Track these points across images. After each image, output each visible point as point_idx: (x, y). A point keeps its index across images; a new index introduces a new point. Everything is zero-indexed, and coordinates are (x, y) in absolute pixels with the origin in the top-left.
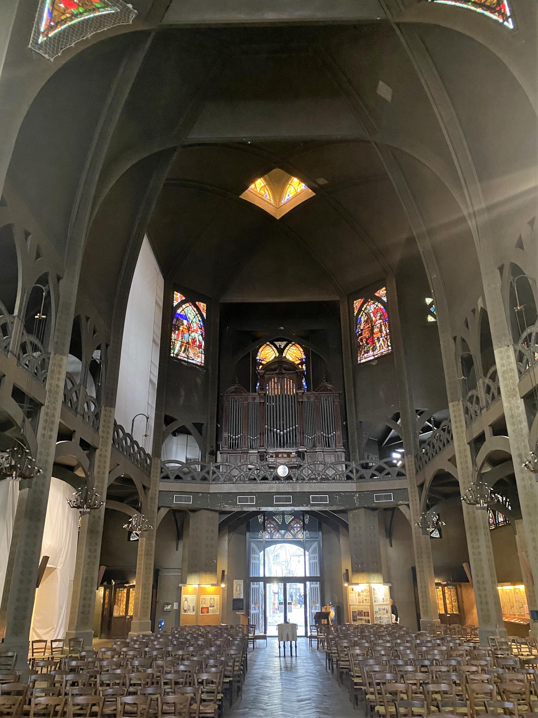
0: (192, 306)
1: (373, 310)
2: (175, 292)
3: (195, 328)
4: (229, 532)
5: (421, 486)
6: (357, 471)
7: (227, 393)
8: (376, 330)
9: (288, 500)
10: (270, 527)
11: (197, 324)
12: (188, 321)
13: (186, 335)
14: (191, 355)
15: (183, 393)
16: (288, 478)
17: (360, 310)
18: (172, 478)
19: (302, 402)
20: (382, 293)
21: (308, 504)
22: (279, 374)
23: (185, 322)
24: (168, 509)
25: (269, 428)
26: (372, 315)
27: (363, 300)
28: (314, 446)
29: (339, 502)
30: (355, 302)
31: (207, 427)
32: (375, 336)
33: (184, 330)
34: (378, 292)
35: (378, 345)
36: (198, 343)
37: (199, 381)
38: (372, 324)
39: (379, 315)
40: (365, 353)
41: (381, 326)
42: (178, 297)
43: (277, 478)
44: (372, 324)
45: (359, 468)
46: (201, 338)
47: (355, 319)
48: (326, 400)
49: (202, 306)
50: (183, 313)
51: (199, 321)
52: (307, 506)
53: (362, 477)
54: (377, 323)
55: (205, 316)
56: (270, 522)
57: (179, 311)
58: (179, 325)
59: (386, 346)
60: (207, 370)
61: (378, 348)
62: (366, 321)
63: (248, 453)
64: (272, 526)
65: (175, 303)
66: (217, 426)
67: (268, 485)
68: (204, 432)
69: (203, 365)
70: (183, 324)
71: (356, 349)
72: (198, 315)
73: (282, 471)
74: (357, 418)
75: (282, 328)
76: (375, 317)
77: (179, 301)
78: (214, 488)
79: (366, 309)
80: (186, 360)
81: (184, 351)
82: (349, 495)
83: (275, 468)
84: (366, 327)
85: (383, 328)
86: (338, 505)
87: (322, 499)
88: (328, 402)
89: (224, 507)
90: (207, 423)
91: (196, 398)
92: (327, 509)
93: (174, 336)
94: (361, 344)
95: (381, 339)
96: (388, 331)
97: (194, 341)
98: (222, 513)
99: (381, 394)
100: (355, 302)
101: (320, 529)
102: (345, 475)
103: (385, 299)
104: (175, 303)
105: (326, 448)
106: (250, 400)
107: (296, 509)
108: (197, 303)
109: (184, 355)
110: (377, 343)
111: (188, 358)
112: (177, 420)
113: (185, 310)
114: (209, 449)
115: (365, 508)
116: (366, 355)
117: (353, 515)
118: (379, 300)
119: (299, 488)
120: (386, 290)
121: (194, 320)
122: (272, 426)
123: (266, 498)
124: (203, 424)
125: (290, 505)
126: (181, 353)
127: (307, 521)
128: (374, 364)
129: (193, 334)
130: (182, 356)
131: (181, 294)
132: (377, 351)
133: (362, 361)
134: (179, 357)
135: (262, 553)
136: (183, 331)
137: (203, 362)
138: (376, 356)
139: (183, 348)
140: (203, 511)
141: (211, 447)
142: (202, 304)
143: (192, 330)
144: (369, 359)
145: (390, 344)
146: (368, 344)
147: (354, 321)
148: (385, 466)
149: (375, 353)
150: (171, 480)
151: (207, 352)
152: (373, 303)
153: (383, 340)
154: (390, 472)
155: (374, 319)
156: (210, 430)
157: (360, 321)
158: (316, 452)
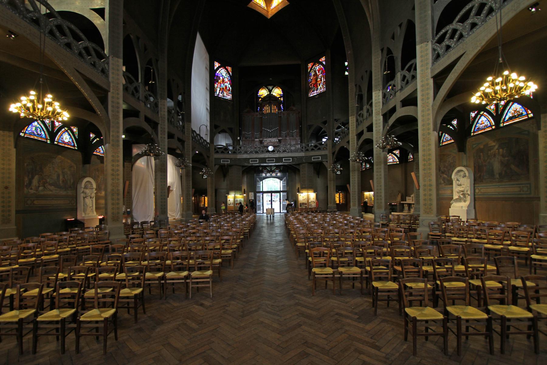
5: (333, 153)
6: (305, 147)
9: (273, 160)
14: (225, 95)
16: (273, 151)
21: (282, 162)
42: (217, 65)
43: (268, 151)
49: (229, 69)
53: (307, 150)
57: (218, 72)
73: (271, 148)
78: (239, 156)
82: (301, 158)
83: (268, 147)
93: (216, 85)
97: (226, 87)
98: (243, 166)
107: (277, 164)
123: (263, 160)
130: (221, 95)
151: (233, 93)
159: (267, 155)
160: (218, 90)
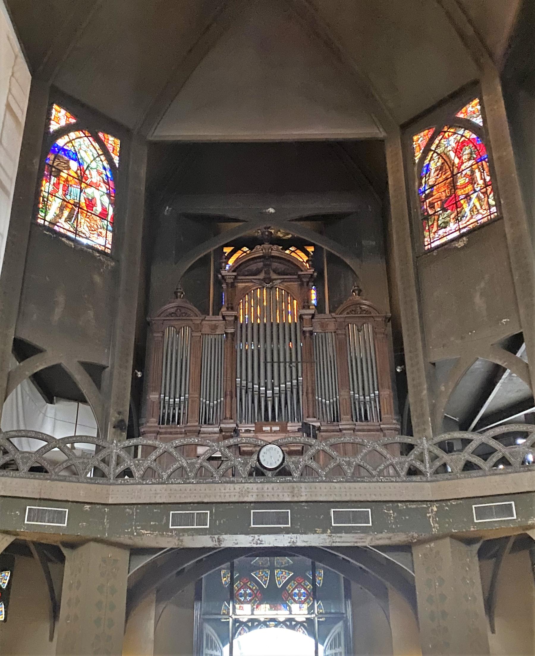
0: (91, 139)
1: (454, 145)
2: (55, 106)
3: (94, 180)
4: (158, 601)
6: (435, 458)
7: (159, 316)
8: (461, 181)
10: (245, 595)
11: (100, 174)
12: (80, 164)
13: (75, 190)
14: (84, 228)
15: (61, 299)
16: (282, 471)
17: (427, 150)
18: (24, 468)
19: (311, 333)
20: (472, 111)
21: (325, 526)
22: (264, 280)
23: (73, 165)
24: (10, 539)
25: (244, 383)
26: (452, 155)
27: (431, 133)
28: (337, 419)
29: (396, 523)
30: (415, 138)
31: (111, 374)
32: (459, 192)
33: (70, 178)
34: (463, 110)
35: (467, 209)
36: (98, 209)
37: (97, 279)
38: (452, 172)
39: (468, 151)
40: (439, 227)
41: (473, 172)
42: (60, 117)
43: (259, 471)
44: (452, 172)
45: (437, 451)
46: (106, 200)
47: (416, 169)
48: (359, 331)
49: (113, 142)
50: (69, 147)
51: (104, 168)
52: (324, 532)
54: (463, 167)
55: (116, 160)
56: (245, 584)
57: (61, 142)
58: (60, 168)
59: (485, 206)
60: (118, 261)
61: (468, 213)
62: (440, 169)
63: (199, 432)
64: (249, 591)
65: (54, 127)
66: (134, 375)
67: (237, 486)
68: (105, 383)
69: (109, 251)
70: (69, 168)
71: (419, 222)
72: (103, 158)
73: (271, 457)
74: (425, 355)
75: (272, 210)
76: (460, 158)
77: (63, 123)
79: (438, 146)
80: (73, 236)
81: (69, 219)
82: (416, 508)
84: (441, 180)
85: (478, 174)
86: (392, 531)
87: (356, 517)
88: (364, 342)
89: (139, 534)
90: (113, 367)
91: (91, 313)
92: (366, 541)
93: (47, 187)
94: (431, 212)
95: (474, 196)
96: (488, 179)
97: (91, 204)
98: (136, 551)
99: (478, 300)
100: (415, 138)
101: (348, 595)
102: (407, 466)
103: (478, 121)
104: (54, 127)
105: (359, 423)
106: (206, 329)
108: (101, 135)
109: (67, 226)
110: (464, 206)
111: (76, 234)
112: (46, 351)
113: (76, 143)
114: (114, 418)
115: (453, 537)
116: (441, 232)
117: (425, 555)
118: (468, 125)
119: (305, 492)
120: (481, 103)
121: (93, 165)
122: (250, 379)
123: (234, 515)
124: (104, 368)
125: (287, 531)
126: (62, 221)
127: (320, 581)
128: (460, 244)
129: (90, 191)
130: (64, 226)
131: (67, 109)
132: (464, 220)
133: (433, 245)
134: (56, 228)
135: (227, 647)
136: (67, 180)
137: (110, 247)
138: (464, 230)
139: (66, 213)
140: (92, 544)
141: (119, 413)
142: (111, 139)
143: (88, 182)
144: (450, 237)
145: (493, 203)
146: (444, 210)
147: (414, 171)
148: (494, 443)
149: (462, 224)
150: (22, 474)
152: (454, 133)
153: (478, 197)
154: (508, 456)
155: (457, 161)
156: (121, 380)
157: (428, 170)
158: (341, 430)
159: (253, 491)
160: (55, 205)
